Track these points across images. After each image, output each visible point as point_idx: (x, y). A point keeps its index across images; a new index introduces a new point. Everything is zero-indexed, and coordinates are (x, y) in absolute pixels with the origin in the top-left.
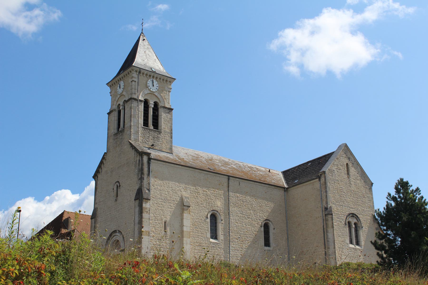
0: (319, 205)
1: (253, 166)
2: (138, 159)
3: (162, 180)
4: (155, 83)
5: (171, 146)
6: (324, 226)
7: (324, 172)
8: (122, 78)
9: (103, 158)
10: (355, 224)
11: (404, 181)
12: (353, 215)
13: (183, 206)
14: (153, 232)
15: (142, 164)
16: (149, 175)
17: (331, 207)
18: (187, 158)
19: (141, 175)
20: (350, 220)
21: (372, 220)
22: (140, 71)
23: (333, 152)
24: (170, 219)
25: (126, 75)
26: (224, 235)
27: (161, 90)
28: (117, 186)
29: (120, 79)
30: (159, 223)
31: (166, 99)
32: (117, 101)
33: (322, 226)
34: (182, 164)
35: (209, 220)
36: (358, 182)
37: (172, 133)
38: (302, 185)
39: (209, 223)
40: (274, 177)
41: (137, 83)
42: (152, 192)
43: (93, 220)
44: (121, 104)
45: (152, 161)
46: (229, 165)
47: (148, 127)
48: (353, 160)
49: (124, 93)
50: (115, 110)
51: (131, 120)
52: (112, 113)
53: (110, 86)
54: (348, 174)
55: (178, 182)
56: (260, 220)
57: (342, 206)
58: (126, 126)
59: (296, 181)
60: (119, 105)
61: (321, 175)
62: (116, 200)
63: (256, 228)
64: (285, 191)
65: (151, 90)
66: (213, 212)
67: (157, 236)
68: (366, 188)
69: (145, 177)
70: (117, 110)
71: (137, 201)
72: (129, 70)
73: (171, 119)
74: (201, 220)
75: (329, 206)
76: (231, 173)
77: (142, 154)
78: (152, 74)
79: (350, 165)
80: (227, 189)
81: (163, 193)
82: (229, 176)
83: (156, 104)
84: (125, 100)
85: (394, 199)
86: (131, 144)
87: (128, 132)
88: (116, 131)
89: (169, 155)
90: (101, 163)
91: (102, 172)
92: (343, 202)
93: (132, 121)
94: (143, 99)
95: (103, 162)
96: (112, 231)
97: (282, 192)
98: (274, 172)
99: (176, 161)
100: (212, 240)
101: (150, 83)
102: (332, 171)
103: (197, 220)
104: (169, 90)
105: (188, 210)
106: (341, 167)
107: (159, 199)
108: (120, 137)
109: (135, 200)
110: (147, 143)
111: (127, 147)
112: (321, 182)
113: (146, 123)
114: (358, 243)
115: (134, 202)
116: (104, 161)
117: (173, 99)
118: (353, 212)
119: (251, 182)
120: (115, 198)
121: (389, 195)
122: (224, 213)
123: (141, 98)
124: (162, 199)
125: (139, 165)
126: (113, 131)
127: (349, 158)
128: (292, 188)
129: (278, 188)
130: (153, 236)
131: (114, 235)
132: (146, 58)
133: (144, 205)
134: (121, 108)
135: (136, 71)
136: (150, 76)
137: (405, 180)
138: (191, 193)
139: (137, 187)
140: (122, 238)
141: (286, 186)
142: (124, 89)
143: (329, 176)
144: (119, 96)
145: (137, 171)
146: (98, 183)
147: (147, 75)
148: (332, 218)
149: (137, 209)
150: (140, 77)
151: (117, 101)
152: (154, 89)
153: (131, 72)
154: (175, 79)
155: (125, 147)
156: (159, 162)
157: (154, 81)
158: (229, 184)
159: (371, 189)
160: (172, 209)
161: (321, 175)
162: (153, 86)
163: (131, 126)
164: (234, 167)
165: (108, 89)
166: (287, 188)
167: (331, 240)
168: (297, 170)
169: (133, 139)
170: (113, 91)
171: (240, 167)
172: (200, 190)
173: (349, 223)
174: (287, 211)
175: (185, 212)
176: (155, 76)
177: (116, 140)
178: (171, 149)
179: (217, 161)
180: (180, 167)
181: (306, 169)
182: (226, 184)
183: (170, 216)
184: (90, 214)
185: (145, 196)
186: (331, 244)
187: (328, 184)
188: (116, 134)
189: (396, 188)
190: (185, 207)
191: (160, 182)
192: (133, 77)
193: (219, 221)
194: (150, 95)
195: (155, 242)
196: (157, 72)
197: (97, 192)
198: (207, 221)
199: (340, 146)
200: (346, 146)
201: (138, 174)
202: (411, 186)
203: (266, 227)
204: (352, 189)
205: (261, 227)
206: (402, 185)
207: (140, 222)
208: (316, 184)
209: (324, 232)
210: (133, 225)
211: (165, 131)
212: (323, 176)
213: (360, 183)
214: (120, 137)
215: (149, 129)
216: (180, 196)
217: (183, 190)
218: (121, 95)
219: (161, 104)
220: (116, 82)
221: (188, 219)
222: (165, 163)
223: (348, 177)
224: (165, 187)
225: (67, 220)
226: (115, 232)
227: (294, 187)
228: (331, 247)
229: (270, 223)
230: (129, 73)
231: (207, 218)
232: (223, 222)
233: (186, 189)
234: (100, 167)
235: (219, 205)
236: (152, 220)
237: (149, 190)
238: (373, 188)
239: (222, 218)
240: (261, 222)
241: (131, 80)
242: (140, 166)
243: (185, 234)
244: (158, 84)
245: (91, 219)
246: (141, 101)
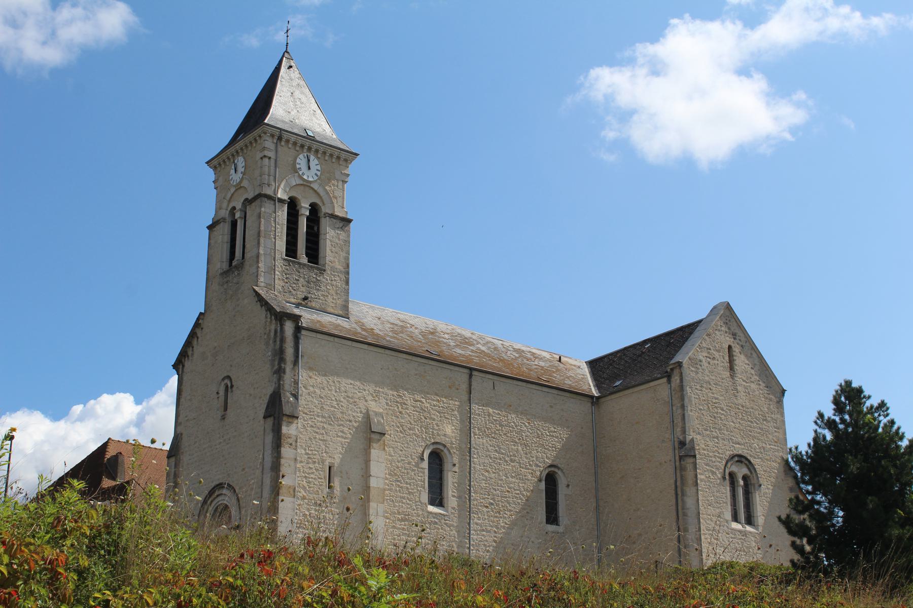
0: (667, 436)
1: (524, 348)
2: (273, 327)
3: (325, 375)
4: (314, 162)
5: (347, 301)
6: (676, 481)
7: (680, 364)
8: (242, 149)
9: (197, 325)
10: (745, 478)
11: (854, 385)
12: (741, 459)
13: (370, 433)
14: (304, 488)
15: (283, 340)
16: (296, 362)
17: (692, 440)
18: (380, 327)
19: (279, 364)
20: (734, 468)
21: (782, 469)
22: (281, 135)
23: (700, 322)
24: (342, 460)
25: (251, 143)
26: (459, 497)
27: (326, 177)
28: (227, 387)
29: (237, 152)
30: (317, 470)
31: (336, 198)
32: (229, 201)
33: (672, 481)
34: (370, 340)
35: (425, 465)
36: (753, 386)
37: (348, 273)
38: (630, 391)
39: (426, 471)
40: (570, 373)
41: (272, 161)
42: (302, 401)
43: (173, 460)
44: (239, 206)
45: (303, 332)
46: (473, 345)
47: (295, 257)
48: (743, 339)
49: (245, 183)
50: (224, 220)
51: (259, 243)
52: (218, 227)
53: (215, 168)
54: (732, 368)
55: (360, 380)
56: (537, 466)
57: (717, 438)
58: (247, 256)
59: (618, 383)
60: (234, 208)
61: (672, 370)
62: (223, 418)
63: (526, 484)
64: (593, 404)
65: (305, 177)
66: (435, 446)
67: (311, 496)
68: (771, 400)
69: (288, 367)
70: (229, 220)
71: (270, 421)
72: (256, 133)
73: (347, 242)
74: (409, 463)
75: (688, 438)
76: (476, 362)
77: (281, 317)
78: (307, 143)
79: (736, 349)
80: (465, 398)
81: (327, 402)
82: (471, 369)
83: (314, 209)
84: (246, 199)
85: (831, 425)
86: (257, 294)
87: (253, 270)
88: (225, 266)
89: (340, 321)
90: (193, 335)
91: (192, 354)
92: (720, 429)
93: (262, 244)
94: (285, 197)
95: (196, 333)
96: (213, 485)
97: (586, 406)
98: (570, 361)
99: (356, 333)
100: (431, 508)
101: (301, 161)
102: (695, 362)
103: (399, 464)
104: (343, 178)
105: (382, 442)
106: (717, 355)
107: (318, 416)
108: (235, 280)
109: (265, 417)
110: (294, 292)
111: (248, 302)
113: (291, 251)
114: (750, 521)
115: (262, 422)
116: (198, 331)
117: (351, 197)
118: (740, 452)
119: (520, 383)
120: (220, 413)
121: (821, 415)
122: (460, 449)
123: (281, 194)
124: (323, 417)
125: (275, 341)
126: (219, 265)
127: (734, 335)
128: (609, 398)
129: (579, 397)
130: (304, 498)
131: (217, 493)
132: (295, 108)
133: (284, 429)
134: (238, 215)
135: (272, 136)
136: (302, 146)
137: (854, 385)
138: (387, 404)
139: (270, 390)
140: (234, 501)
141: (595, 392)
142: (244, 173)
143: (689, 372)
145: (270, 353)
146: (185, 378)
147: (295, 144)
148: (695, 464)
149: (269, 438)
150: (279, 149)
151: (229, 201)
152: (309, 176)
153: (260, 136)
154: (357, 155)
155: (246, 301)
156: (319, 336)
157: (312, 158)
158: (470, 385)
159: (780, 403)
160: (346, 438)
161: (672, 370)
162: (309, 168)
163: (258, 256)
164: (483, 348)
165: (210, 174)
166: (598, 398)
167: (691, 513)
168: (620, 358)
169: (262, 284)
170: (221, 179)
171: (496, 349)
172: (408, 398)
173: (732, 475)
174: (596, 449)
175: (374, 445)
176: (314, 147)
177: (225, 286)
178: (346, 307)
179: (446, 336)
180: (366, 346)
181: (640, 356)
182: (464, 386)
183: (341, 453)
184: (167, 447)
185: (287, 410)
186: (691, 520)
187: (688, 390)
188: (225, 274)
189: (836, 401)
190: (373, 436)
191: (320, 379)
192: (264, 148)
193: (447, 466)
194: (302, 187)
195: (308, 510)
196: (318, 138)
197: (182, 400)
198: (421, 466)
199: (715, 308)
200: (728, 307)
201: (273, 361)
202: (869, 397)
203: (551, 481)
204: (740, 401)
205: (540, 480)
206: (849, 396)
207: (276, 467)
208: (661, 388)
209: (677, 495)
210: (258, 472)
211: (333, 269)
212: (676, 372)
213: (757, 388)
214: (235, 280)
215: (299, 264)
216: (364, 411)
217: (369, 398)
218: (239, 187)
219: (325, 209)
220: (228, 158)
221: (380, 460)
222: (331, 339)
223: (732, 377)
224: (330, 390)
225: (116, 458)
226: (220, 486)
227: (613, 396)
228: (692, 529)
229: (559, 472)
230: (255, 140)
231: (422, 459)
232: (456, 469)
233: (376, 396)
234: (188, 344)
235: (449, 431)
236: (301, 462)
237: (296, 396)
238: (786, 400)
239: (456, 460)
240: (539, 471)
241: (262, 155)
242: (278, 343)
243: (373, 493)
244: (321, 164)
245: (168, 457)
246: (281, 201)
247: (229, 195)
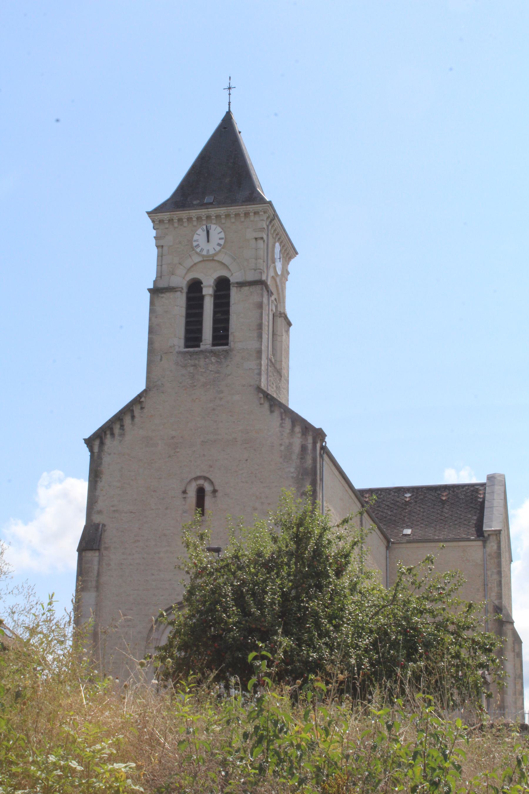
32: (189, 270)
38: (433, 544)
91: (122, 435)
112: (488, 550)
128: (404, 545)
144: (196, 259)
146: (106, 459)
151: (189, 270)
214: (211, 367)
227: (408, 545)
247: (189, 263)
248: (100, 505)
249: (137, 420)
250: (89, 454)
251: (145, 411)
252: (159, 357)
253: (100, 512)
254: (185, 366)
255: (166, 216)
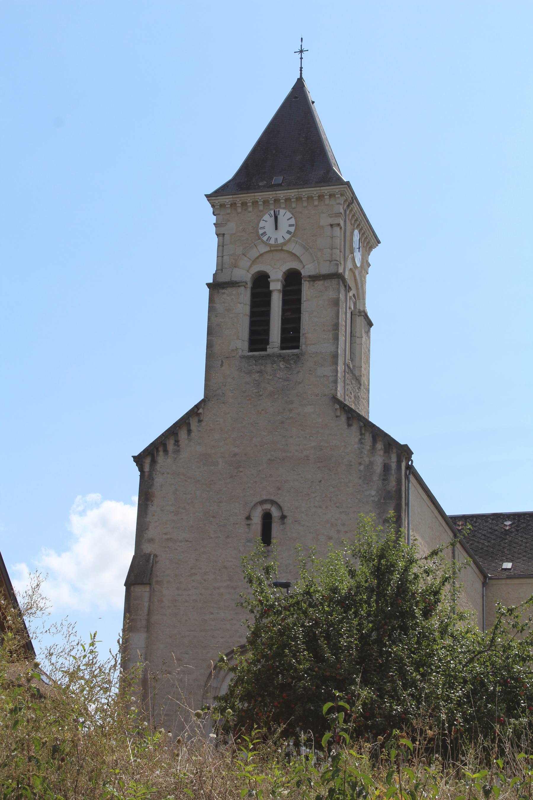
32: (254, 261)
91: (177, 452)
128: (503, 582)
144: (263, 249)
146: (158, 480)
151: (254, 261)
214: (280, 374)
227: (509, 581)
247: (254, 253)
248: (151, 533)
249: (193, 434)
250: (139, 473)
251: (203, 424)
252: (220, 363)
253: (151, 541)
254: (249, 373)
255: (227, 199)
